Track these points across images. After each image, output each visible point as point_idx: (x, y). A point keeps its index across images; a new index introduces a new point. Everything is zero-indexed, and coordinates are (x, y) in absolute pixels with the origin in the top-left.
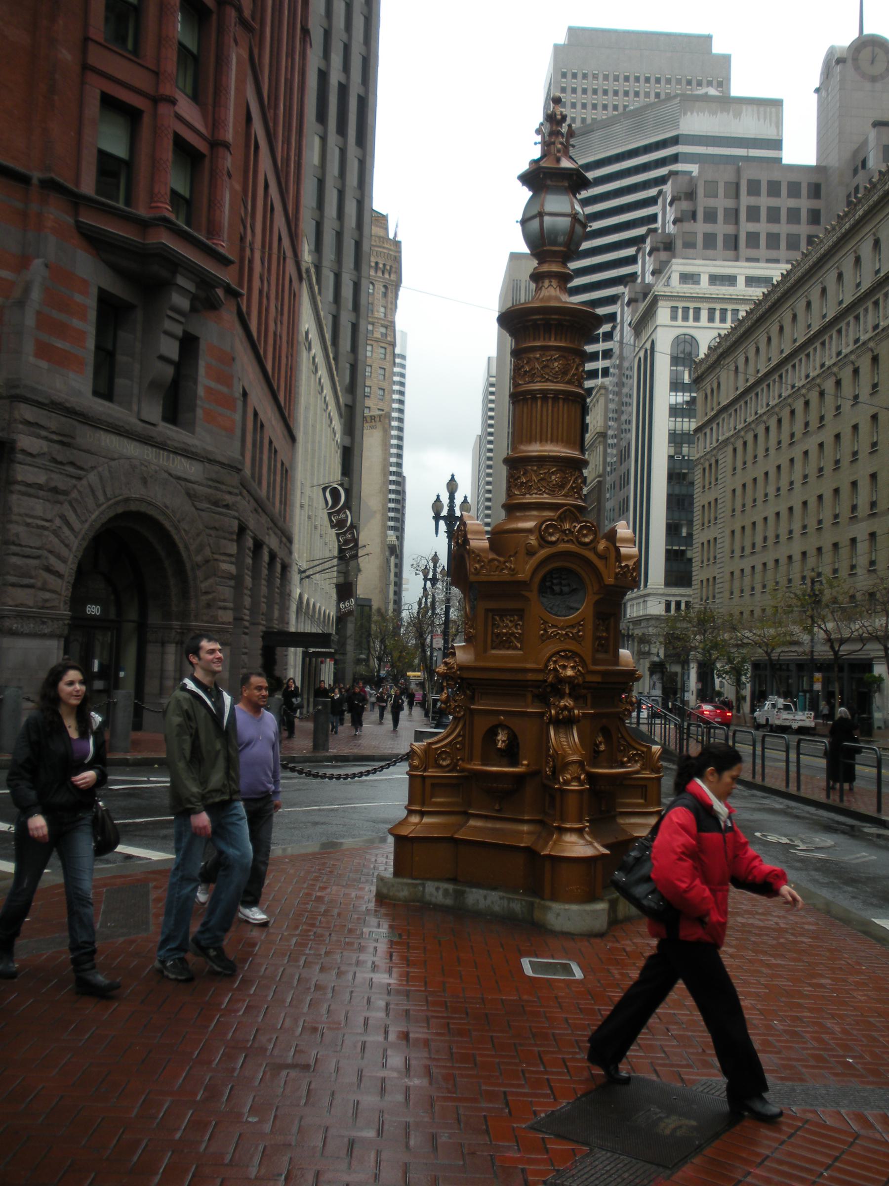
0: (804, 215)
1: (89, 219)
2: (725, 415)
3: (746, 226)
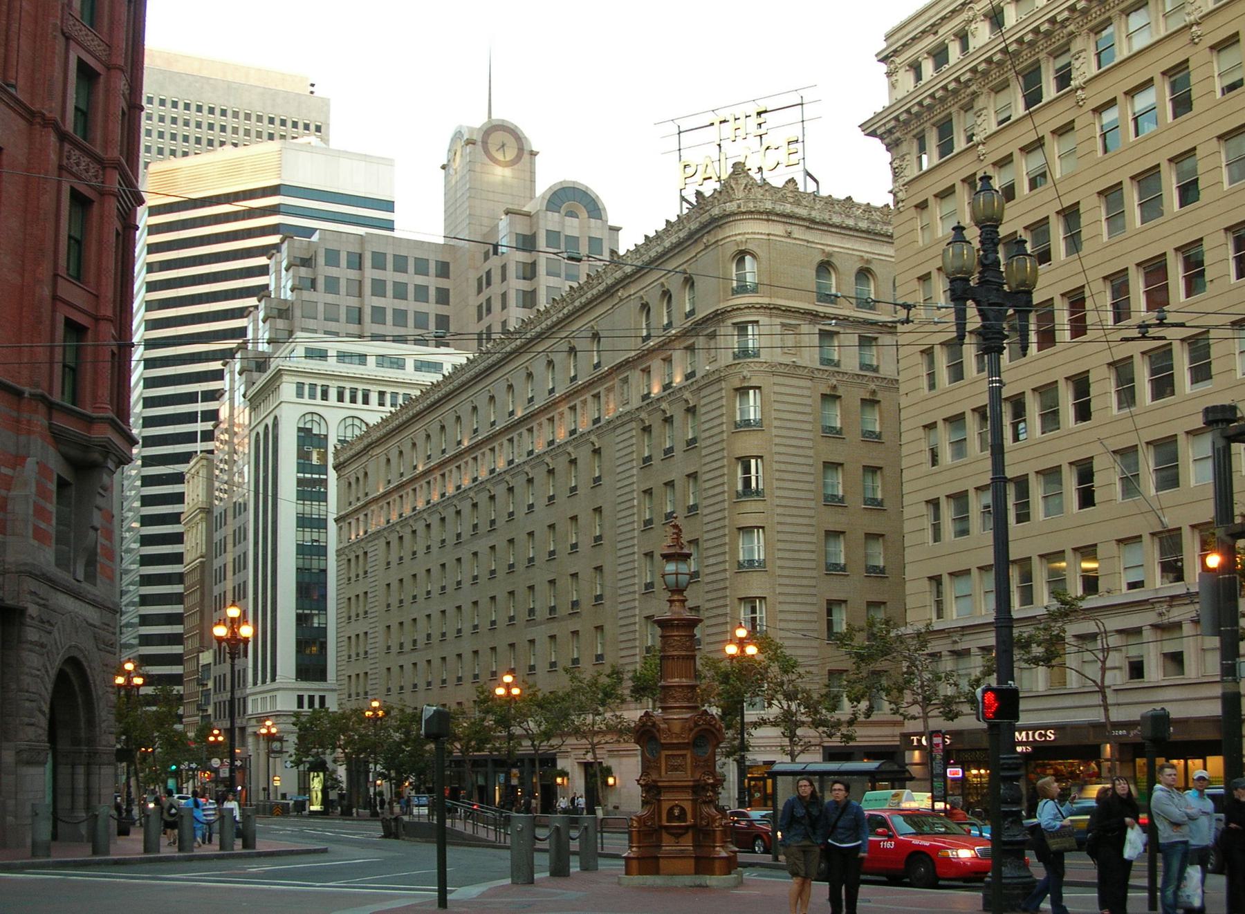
0: (432, 293)
1: (60, 421)
2: (374, 507)
3: (371, 301)
